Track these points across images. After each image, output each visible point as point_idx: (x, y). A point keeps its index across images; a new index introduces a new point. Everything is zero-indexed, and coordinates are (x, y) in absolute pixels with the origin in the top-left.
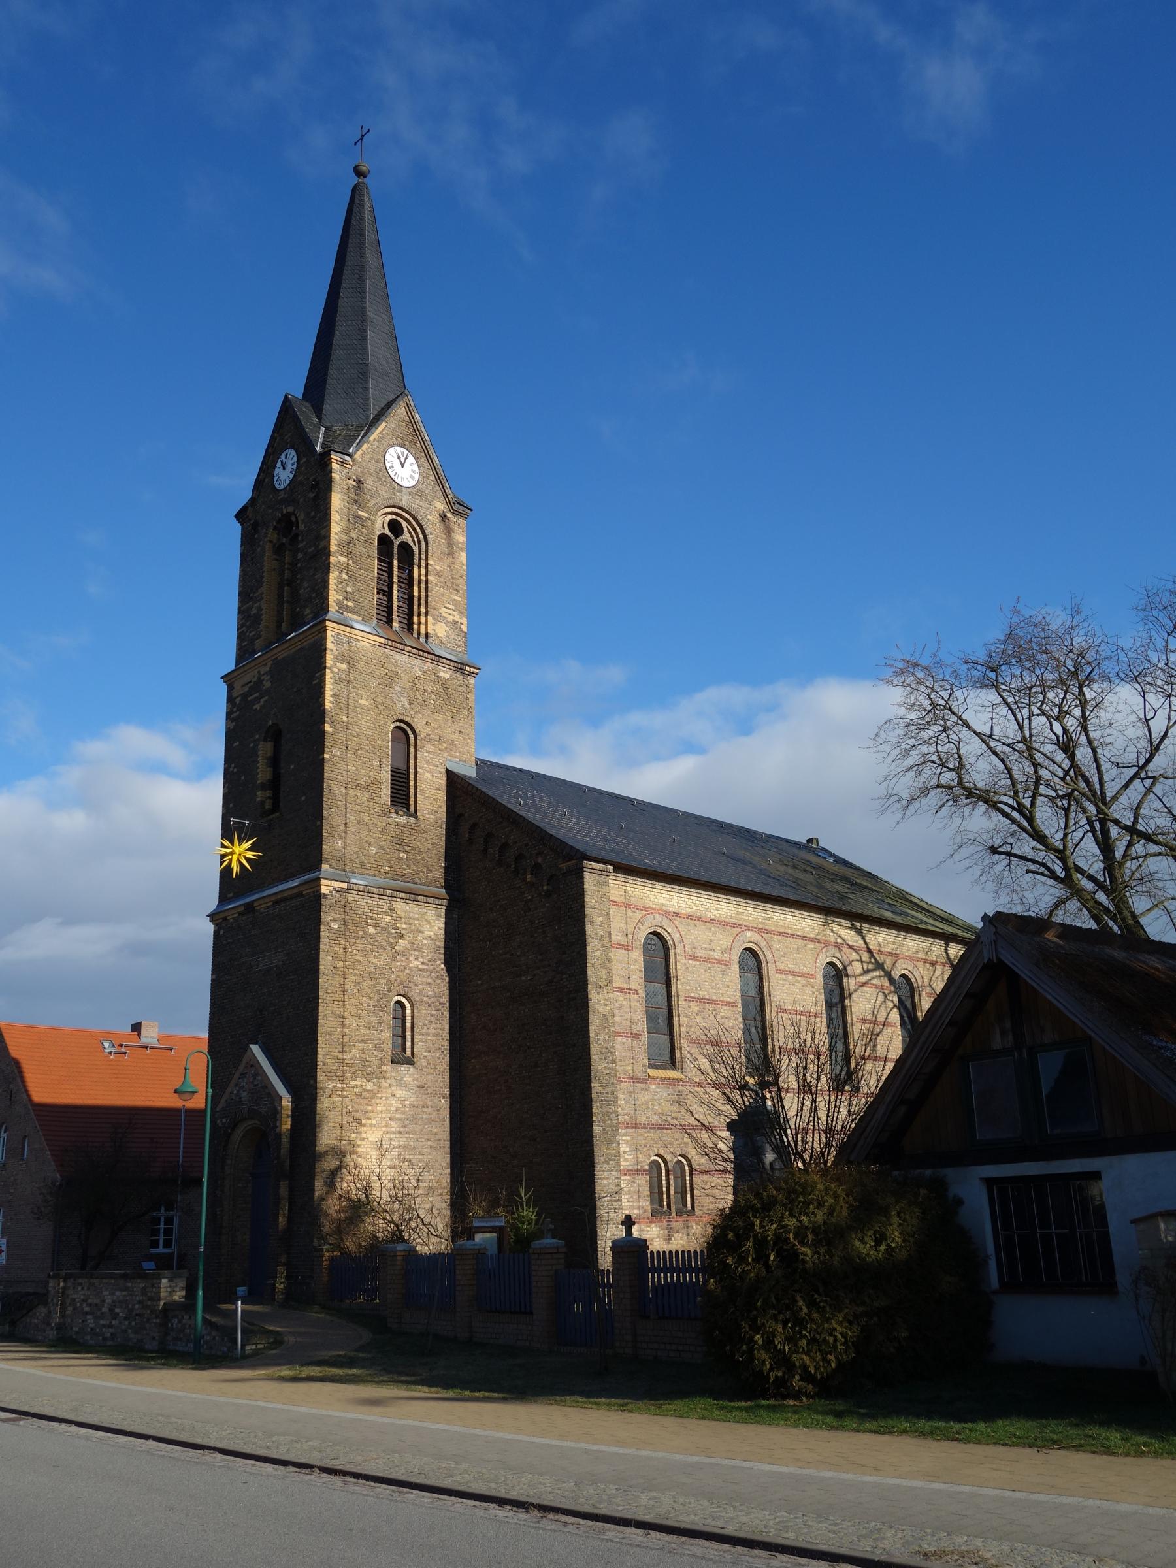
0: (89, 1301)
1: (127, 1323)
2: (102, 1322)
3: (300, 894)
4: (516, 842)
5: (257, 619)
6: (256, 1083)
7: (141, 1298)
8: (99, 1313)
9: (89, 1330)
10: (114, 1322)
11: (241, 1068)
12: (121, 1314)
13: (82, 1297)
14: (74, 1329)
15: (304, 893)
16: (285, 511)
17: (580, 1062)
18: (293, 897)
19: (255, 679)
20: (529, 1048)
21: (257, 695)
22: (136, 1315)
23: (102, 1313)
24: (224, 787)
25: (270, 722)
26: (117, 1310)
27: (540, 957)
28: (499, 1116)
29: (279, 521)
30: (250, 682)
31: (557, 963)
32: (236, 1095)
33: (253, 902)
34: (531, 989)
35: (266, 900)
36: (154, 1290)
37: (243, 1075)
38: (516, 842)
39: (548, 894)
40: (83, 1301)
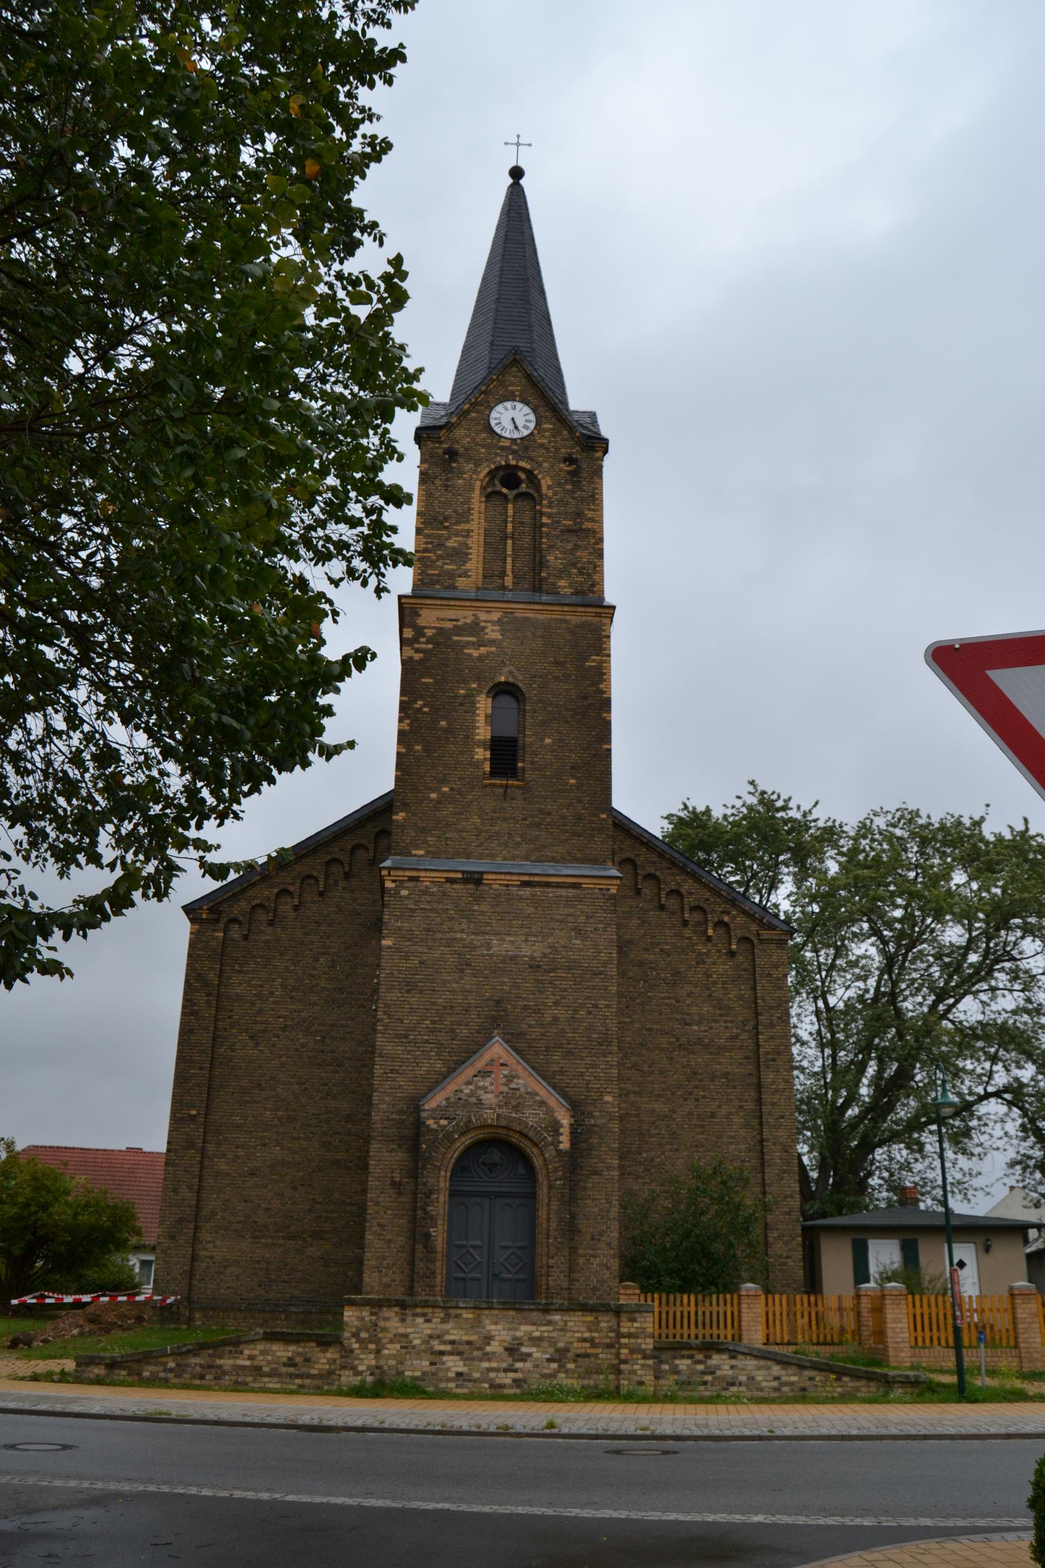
0: (448, 1337)
1: (554, 1365)
2: (485, 1365)
3: (576, 886)
4: (692, 894)
5: (460, 555)
6: (513, 1086)
7: (587, 1335)
8: (477, 1353)
9: (452, 1375)
10: (519, 1365)
11: (480, 1064)
12: (535, 1355)
13: (429, 1332)
16: (513, 463)
18: (558, 885)
19: (469, 621)
20: (703, 1097)
21: (473, 639)
22: (578, 1356)
23: (487, 1354)
24: (401, 720)
25: (503, 679)
26: (524, 1350)
27: (719, 1012)
28: (658, 1160)
29: (499, 468)
30: (457, 620)
31: (742, 1022)
32: (472, 1094)
33: (482, 873)
35: (509, 877)
36: (636, 1325)
37: (484, 1074)
38: (692, 894)
39: (732, 954)
40: (431, 1337)
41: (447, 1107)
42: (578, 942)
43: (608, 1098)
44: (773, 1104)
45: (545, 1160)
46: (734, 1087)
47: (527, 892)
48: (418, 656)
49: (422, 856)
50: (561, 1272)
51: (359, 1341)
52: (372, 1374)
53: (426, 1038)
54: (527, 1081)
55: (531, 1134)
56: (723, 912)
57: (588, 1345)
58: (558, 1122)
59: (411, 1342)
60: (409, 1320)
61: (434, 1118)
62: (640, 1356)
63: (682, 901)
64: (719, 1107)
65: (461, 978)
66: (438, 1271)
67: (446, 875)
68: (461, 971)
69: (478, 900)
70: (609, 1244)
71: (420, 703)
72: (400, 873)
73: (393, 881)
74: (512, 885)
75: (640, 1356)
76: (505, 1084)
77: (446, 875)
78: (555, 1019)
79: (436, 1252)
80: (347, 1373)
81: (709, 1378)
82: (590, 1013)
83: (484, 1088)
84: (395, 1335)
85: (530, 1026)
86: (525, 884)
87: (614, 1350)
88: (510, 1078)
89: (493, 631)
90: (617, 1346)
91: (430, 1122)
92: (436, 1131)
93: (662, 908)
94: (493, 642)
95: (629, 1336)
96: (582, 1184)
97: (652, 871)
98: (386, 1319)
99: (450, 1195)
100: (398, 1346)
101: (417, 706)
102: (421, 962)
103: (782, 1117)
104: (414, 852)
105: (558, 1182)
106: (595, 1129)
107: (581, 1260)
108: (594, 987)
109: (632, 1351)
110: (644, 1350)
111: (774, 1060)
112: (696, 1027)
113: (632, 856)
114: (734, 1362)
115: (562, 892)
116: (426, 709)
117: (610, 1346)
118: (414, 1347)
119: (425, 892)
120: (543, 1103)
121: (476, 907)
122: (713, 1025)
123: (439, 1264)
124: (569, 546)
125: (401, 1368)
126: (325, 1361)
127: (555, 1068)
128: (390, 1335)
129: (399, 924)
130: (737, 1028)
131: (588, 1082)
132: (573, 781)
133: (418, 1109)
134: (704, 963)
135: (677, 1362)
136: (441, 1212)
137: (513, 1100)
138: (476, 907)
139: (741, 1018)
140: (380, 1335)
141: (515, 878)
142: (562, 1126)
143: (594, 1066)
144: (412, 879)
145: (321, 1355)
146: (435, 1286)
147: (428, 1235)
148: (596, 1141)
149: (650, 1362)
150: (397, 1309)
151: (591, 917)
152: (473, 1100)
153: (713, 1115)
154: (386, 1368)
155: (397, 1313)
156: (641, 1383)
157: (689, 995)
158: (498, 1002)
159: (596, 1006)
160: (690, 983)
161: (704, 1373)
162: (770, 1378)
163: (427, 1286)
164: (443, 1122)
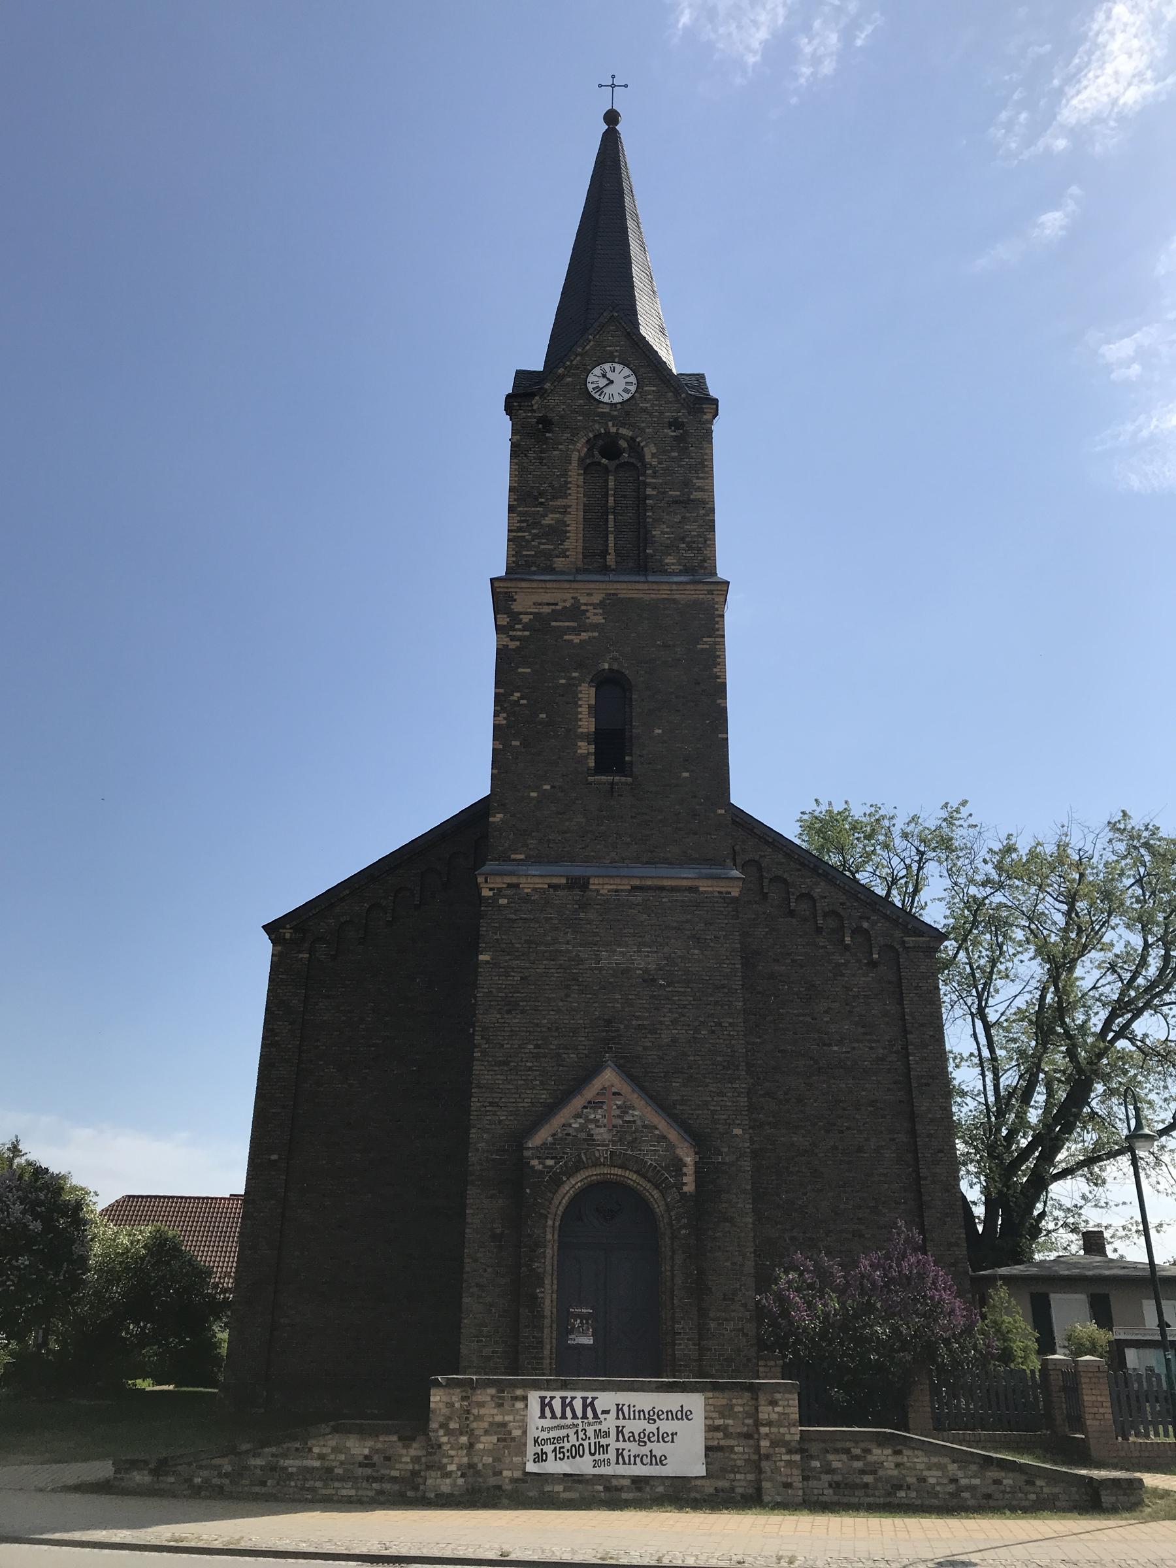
5: (558, 533)
6: (627, 1118)
7: (721, 1422)
11: (590, 1092)
14: (506, 1473)
15: (701, 889)
16: (613, 430)
17: (941, 1155)
18: (673, 889)
19: (568, 605)
20: (848, 1128)
24: (496, 714)
25: (606, 666)
27: (862, 1030)
32: (582, 1128)
34: (849, 1063)
35: (618, 881)
36: (777, 1409)
37: (594, 1105)
39: (873, 964)
41: (554, 1144)
42: (697, 952)
43: (738, 1131)
44: (929, 1136)
45: (667, 1205)
46: (883, 1117)
47: (639, 898)
48: (514, 645)
49: (521, 860)
50: (688, 1339)
51: (449, 1432)
52: (463, 1475)
53: (529, 1064)
54: (643, 1112)
55: (650, 1174)
56: (861, 918)
57: (721, 1435)
58: (681, 1160)
59: (510, 1433)
60: (507, 1407)
61: (539, 1158)
62: (783, 1450)
63: (815, 906)
64: (867, 1140)
65: (567, 996)
66: (547, 1341)
67: (548, 881)
68: (567, 987)
69: (583, 906)
70: (745, 1305)
71: (518, 695)
72: (498, 879)
73: (491, 889)
74: (622, 890)
75: (783, 1450)
76: (619, 1117)
77: (548, 881)
78: (674, 1040)
79: (543, 1317)
80: (433, 1474)
81: (868, 1479)
82: (713, 1032)
83: (596, 1121)
84: (491, 1424)
85: (645, 1048)
86: (635, 888)
87: (751, 1442)
88: (624, 1109)
89: (595, 614)
90: (756, 1436)
91: (534, 1162)
92: (541, 1172)
93: (792, 913)
94: (595, 627)
95: (770, 1424)
96: (710, 1233)
97: (780, 873)
98: (481, 1405)
99: (559, 1248)
100: (494, 1439)
101: (512, 698)
102: (522, 978)
103: (941, 1151)
104: (513, 856)
105: (683, 1232)
106: (724, 1167)
107: (712, 1325)
108: (716, 1003)
109: (774, 1444)
110: (789, 1442)
111: (928, 1085)
112: (836, 1048)
113: (757, 858)
114: (899, 1459)
115: (677, 896)
116: (523, 702)
117: (748, 1436)
118: (513, 1439)
119: (526, 899)
120: (663, 1138)
121: (582, 915)
122: (856, 1045)
123: (546, 1331)
124: (677, 519)
125: (498, 1467)
126: (408, 1459)
127: (675, 1097)
128: (486, 1425)
129: (498, 937)
130: (884, 1048)
131: (714, 1112)
132: (686, 775)
133: (521, 1147)
134: (842, 975)
135: (830, 1457)
136: (549, 1268)
137: (628, 1134)
138: (582, 915)
139: (887, 1038)
140: (474, 1425)
141: (625, 881)
142: (685, 1165)
143: (721, 1094)
144: (510, 886)
145: (404, 1452)
146: (542, 1358)
147: (534, 1297)
148: (725, 1181)
149: (797, 1457)
150: (492, 1391)
151: (711, 924)
152: (583, 1136)
153: (860, 1149)
154: (480, 1466)
155: (492, 1397)
156: (787, 1486)
157: (826, 1012)
158: (609, 1022)
159: (719, 1024)
160: (828, 998)
161: (863, 1472)
162: (945, 1481)
163: (535, 1358)
164: (550, 1162)
